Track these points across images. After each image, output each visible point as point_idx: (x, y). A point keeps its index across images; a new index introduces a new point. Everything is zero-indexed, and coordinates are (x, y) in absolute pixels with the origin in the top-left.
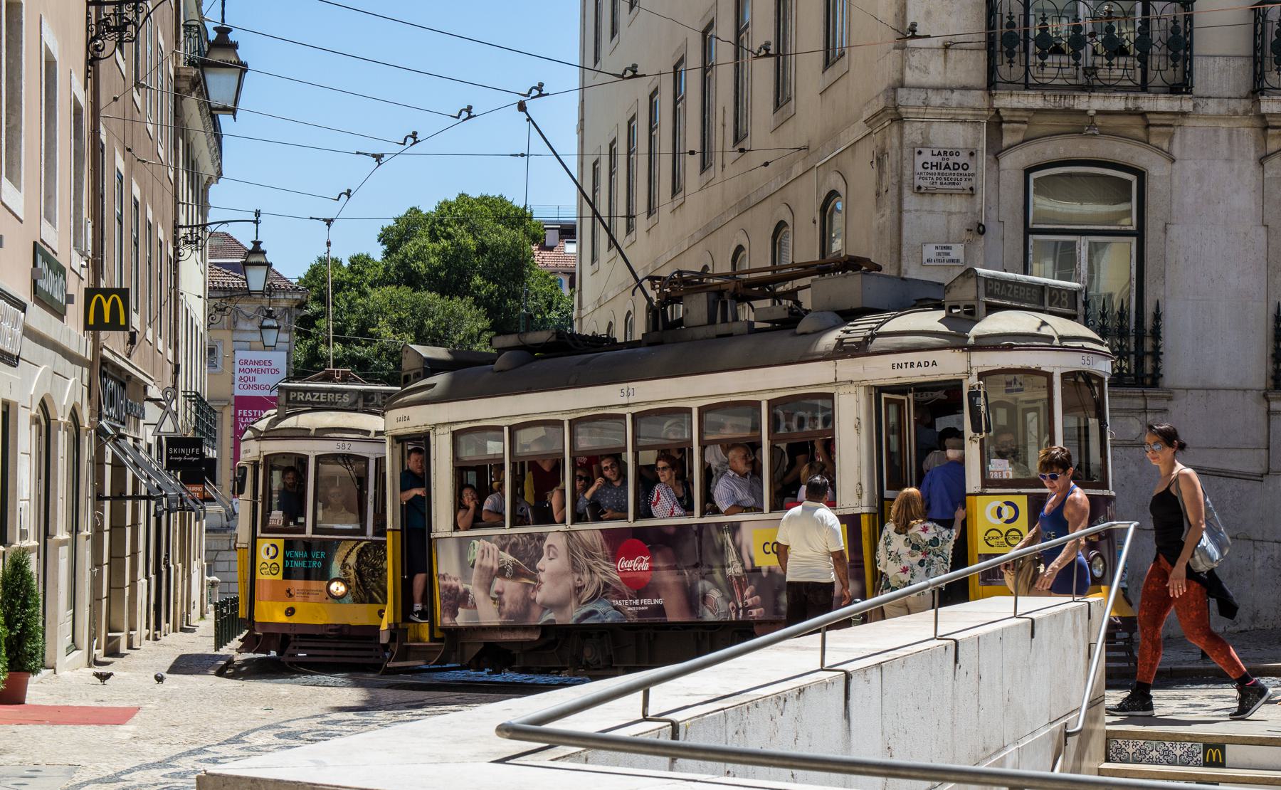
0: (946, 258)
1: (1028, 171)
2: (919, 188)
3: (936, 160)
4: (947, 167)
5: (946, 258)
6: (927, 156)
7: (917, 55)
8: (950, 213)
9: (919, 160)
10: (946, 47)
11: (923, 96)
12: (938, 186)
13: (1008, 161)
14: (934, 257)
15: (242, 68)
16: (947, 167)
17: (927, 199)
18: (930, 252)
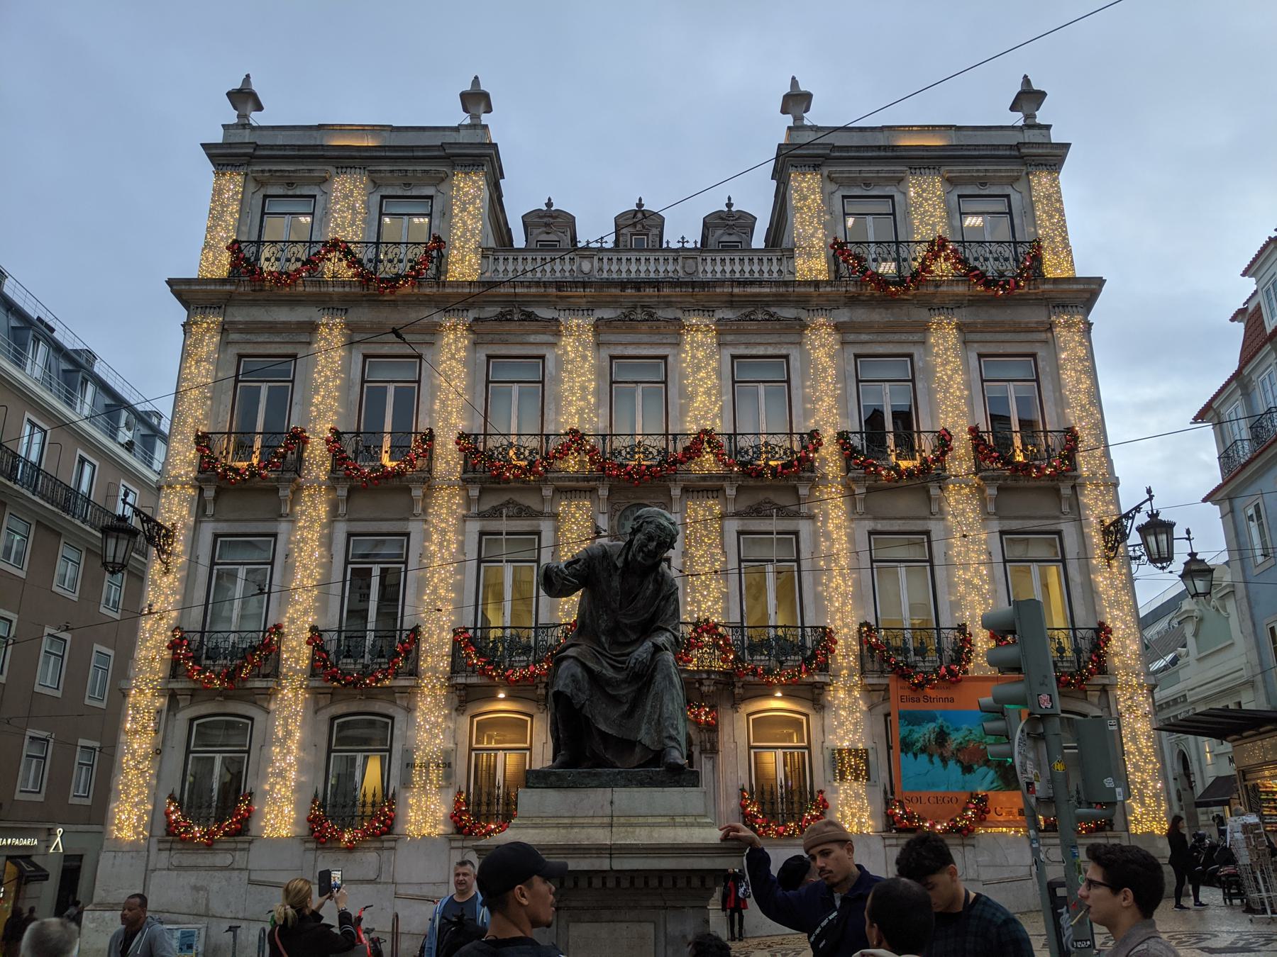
1: (192, 720)
13: (179, 716)
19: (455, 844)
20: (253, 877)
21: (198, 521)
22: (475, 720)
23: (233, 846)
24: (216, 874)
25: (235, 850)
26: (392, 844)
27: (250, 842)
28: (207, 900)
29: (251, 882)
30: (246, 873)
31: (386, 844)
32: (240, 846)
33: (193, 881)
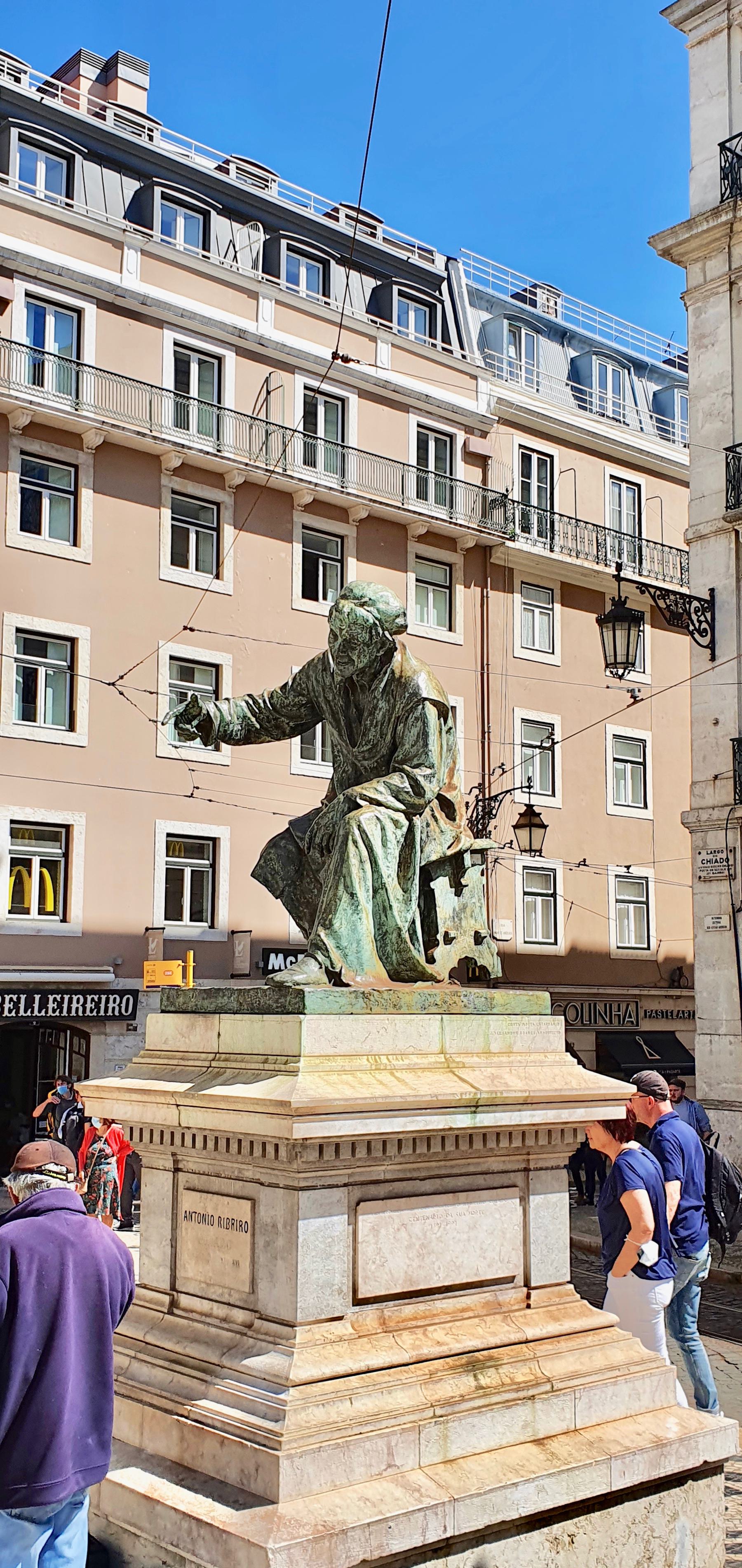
0: (719, 925)
2: (700, 877)
3: (710, 857)
4: (716, 861)
5: (719, 925)
6: (704, 855)
7: (697, 786)
8: (721, 894)
9: (700, 858)
10: (716, 777)
11: (697, 814)
12: (711, 875)
14: (711, 925)
15: (545, 827)
16: (716, 861)
17: (708, 884)
18: (709, 922)
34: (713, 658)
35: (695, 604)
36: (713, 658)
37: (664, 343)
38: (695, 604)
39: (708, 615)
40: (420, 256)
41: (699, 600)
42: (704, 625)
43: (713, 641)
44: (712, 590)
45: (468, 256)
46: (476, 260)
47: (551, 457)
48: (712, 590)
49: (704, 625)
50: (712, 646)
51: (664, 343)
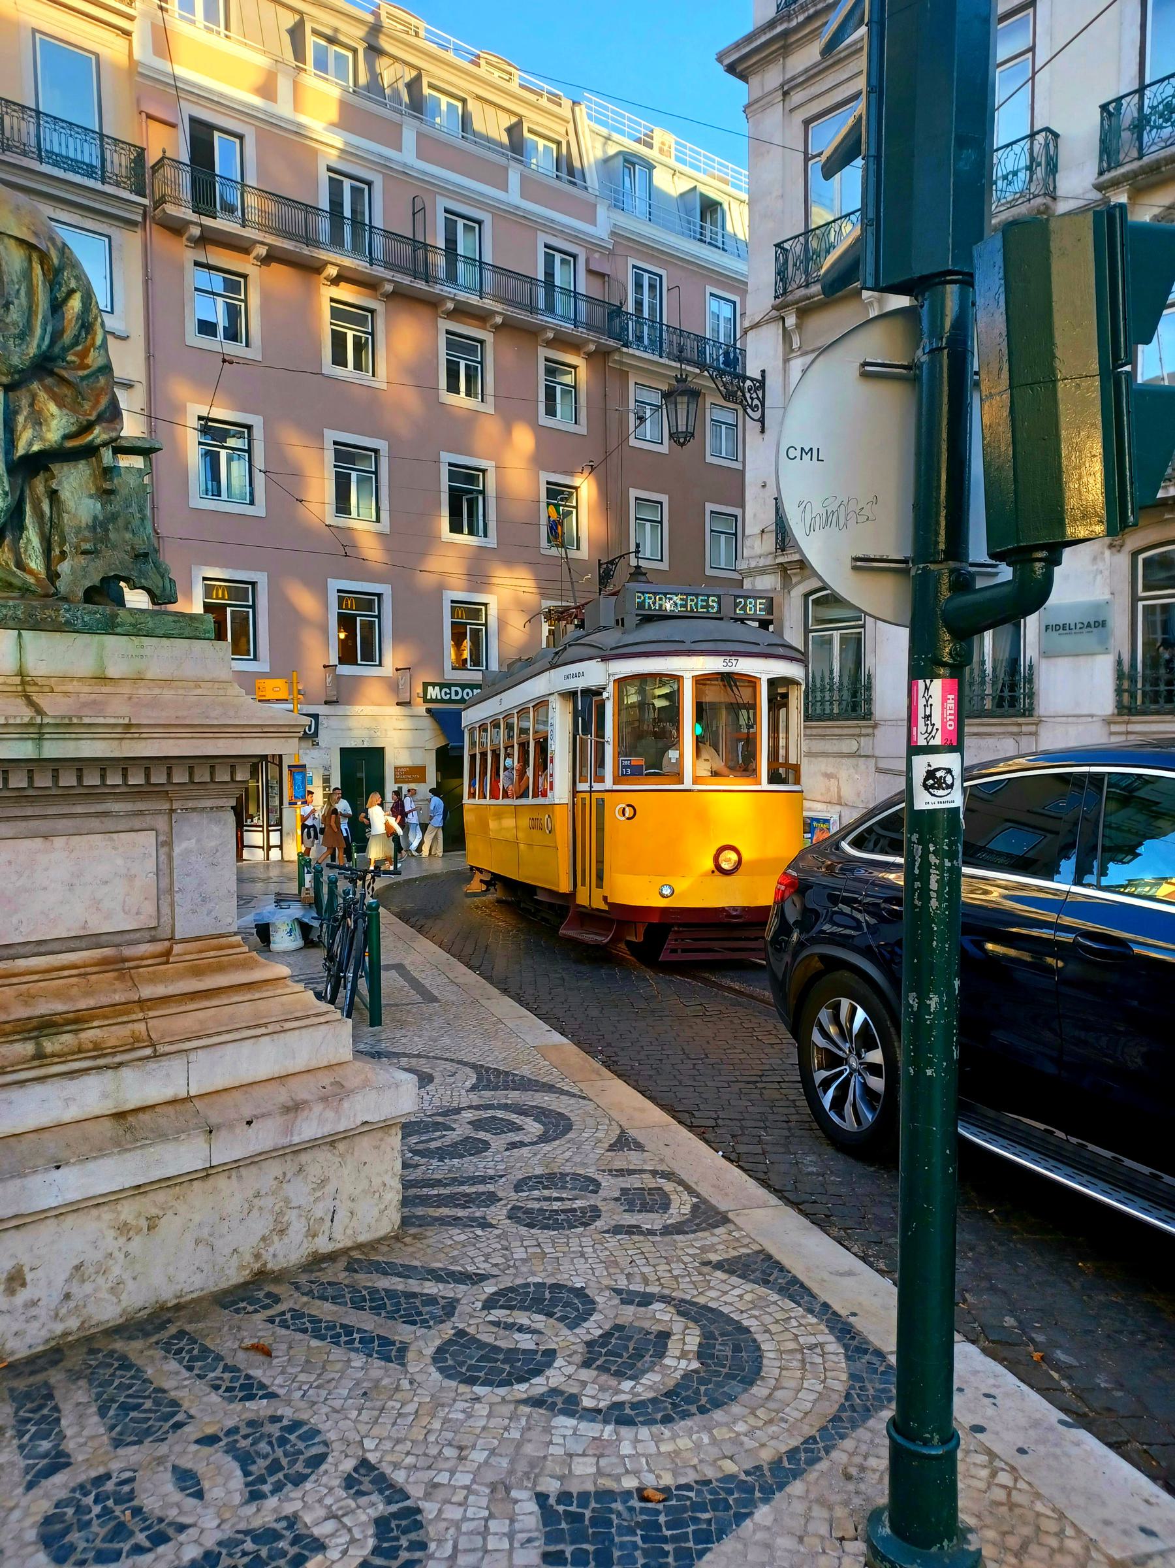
1: (806, 596)
13: (793, 593)
19: (1114, 728)
20: (880, 765)
21: (786, 361)
22: (1141, 557)
23: (857, 731)
24: (844, 760)
25: (860, 735)
26: (1033, 728)
27: (874, 727)
28: (839, 788)
29: (879, 770)
30: (873, 761)
31: (1025, 729)
32: (864, 731)
33: (823, 768)
34: (763, 431)
35: (748, 383)
36: (763, 431)
37: (645, 127)
38: (748, 383)
39: (760, 393)
40: (549, 100)
41: (752, 380)
42: (756, 402)
43: (763, 415)
44: (763, 372)
45: (590, 101)
46: (597, 104)
47: (370, 184)
48: (763, 372)
49: (756, 402)
50: (762, 420)
51: (645, 127)
